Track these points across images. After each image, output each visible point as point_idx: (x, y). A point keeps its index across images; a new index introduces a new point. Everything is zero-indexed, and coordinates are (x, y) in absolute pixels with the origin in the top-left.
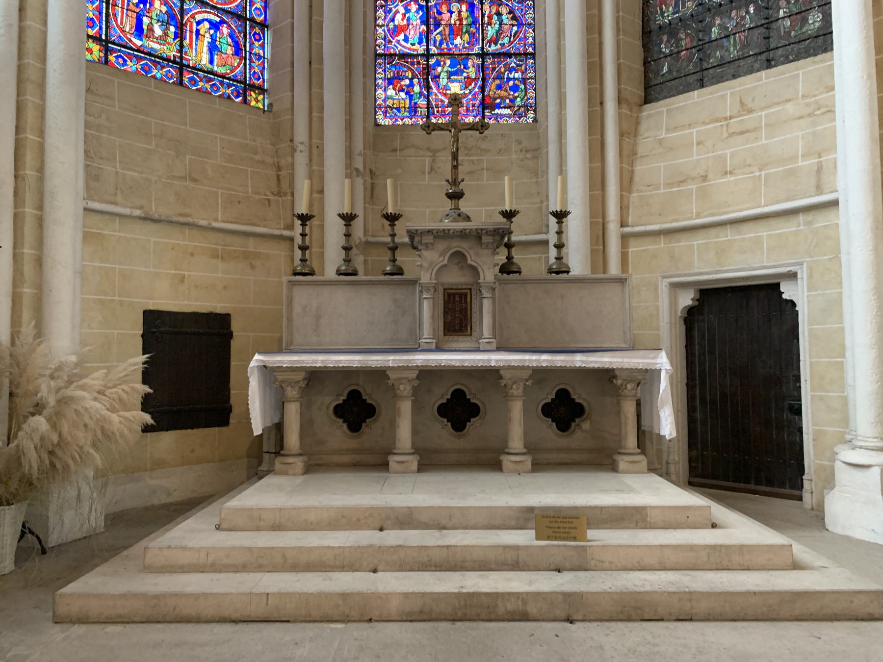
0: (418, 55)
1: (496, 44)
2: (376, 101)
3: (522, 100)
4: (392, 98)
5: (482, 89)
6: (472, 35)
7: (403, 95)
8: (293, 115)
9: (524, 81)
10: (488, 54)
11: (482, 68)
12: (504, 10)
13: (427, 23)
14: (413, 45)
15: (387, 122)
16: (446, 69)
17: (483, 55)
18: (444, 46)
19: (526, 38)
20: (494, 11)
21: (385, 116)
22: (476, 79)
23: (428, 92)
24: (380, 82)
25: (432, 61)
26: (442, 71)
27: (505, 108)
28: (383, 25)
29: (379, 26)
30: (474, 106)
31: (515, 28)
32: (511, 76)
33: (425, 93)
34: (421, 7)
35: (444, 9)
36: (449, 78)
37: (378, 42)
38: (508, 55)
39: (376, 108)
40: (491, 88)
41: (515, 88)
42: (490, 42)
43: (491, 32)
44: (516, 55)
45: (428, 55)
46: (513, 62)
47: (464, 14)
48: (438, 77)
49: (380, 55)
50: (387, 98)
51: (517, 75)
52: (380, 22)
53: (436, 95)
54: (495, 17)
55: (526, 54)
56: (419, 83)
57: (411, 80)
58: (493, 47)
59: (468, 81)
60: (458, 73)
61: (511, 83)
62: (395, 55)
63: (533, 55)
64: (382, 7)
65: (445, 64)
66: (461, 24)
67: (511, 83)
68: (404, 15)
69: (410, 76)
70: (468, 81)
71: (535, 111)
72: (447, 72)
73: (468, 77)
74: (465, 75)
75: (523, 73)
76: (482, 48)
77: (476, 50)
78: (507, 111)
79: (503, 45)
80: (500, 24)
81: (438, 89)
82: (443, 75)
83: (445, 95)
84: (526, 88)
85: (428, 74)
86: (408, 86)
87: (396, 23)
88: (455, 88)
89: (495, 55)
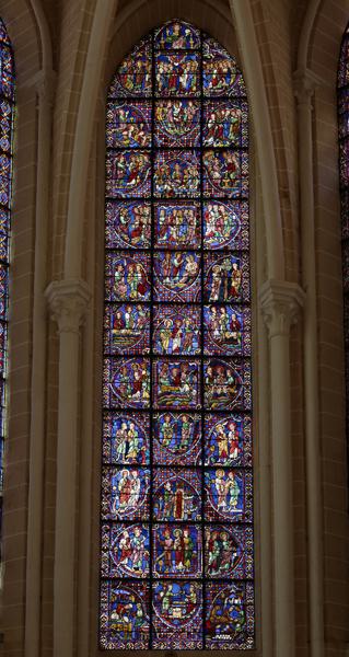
0: (141, 580)
1: (216, 570)
2: (100, 624)
3: (242, 625)
4: (115, 621)
5: (203, 614)
6: (194, 561)
7: (126, 619)
8: (23, 648)
9: (244, 607)
10: (209, 580)
11: (204, 593)
12: (224, 537)
13: (151, 550)
14: (137, 569)
15: (111, 646)
16: (168, 594)
17: (204, 580)
18: (167, 571)
19: (245, 564)
20: (215, 537)
21: (108, 640)
22: (197, 605)
23: (151, 617)
24: (104, 605)
25: (156, 586)
26: (165, 596)
27: (225, 633)
28: (108, 549)
29: (103, 550)
30: (195, 630)
31: (235, 554)
32: (231, 602)
33: (148, 617)
34: (144, 533)
35: (167, 534)
36: (171, 603)
37: (103, 566)
38: (230, 581)
39: (101, 632)
40: (212, 612)
41: (235, 613)
42: (210, 567)
43: (211, 558)
44: (236, 581)
45: (150, 579)
46: (233, 588)
47: (186, 540)
48: (161, 601)
49: (105, 579)
50: (111, 621)
51: (236, 602)
52: (105, 546)
53: (159, 619)
54: (216, 544)
55: (245, 581)
56: (142, 607)
57: (134, 604)
58: (214, 574)
59: (190, 606)
60: (181, 598)
61: (231, 609)
62: (117, 580)
63: (252, 581)
64: (108, 531)
65: (167, 589)
66: (183, 550)
67: (231, 609)
68: (128, 539)
69: (133, 600)
70: (190, 606)
71: (254, 637)
72: (170, 596)
73: (190, 603)
74: (187, 600)
75: (242, 599)
76: (204, 574)
77: (198, 574)
78: (228, 637)
79: (223, 571)
80: (221, 551)
81: (160, 612)
82: (165, 600)
83: (167, 619)
84: (245, 614)
85: (151, 598)
86: (131, 610)
87: (121, 547)
88: (177, 613)
89: (216, 581)
